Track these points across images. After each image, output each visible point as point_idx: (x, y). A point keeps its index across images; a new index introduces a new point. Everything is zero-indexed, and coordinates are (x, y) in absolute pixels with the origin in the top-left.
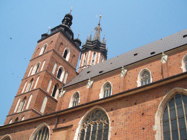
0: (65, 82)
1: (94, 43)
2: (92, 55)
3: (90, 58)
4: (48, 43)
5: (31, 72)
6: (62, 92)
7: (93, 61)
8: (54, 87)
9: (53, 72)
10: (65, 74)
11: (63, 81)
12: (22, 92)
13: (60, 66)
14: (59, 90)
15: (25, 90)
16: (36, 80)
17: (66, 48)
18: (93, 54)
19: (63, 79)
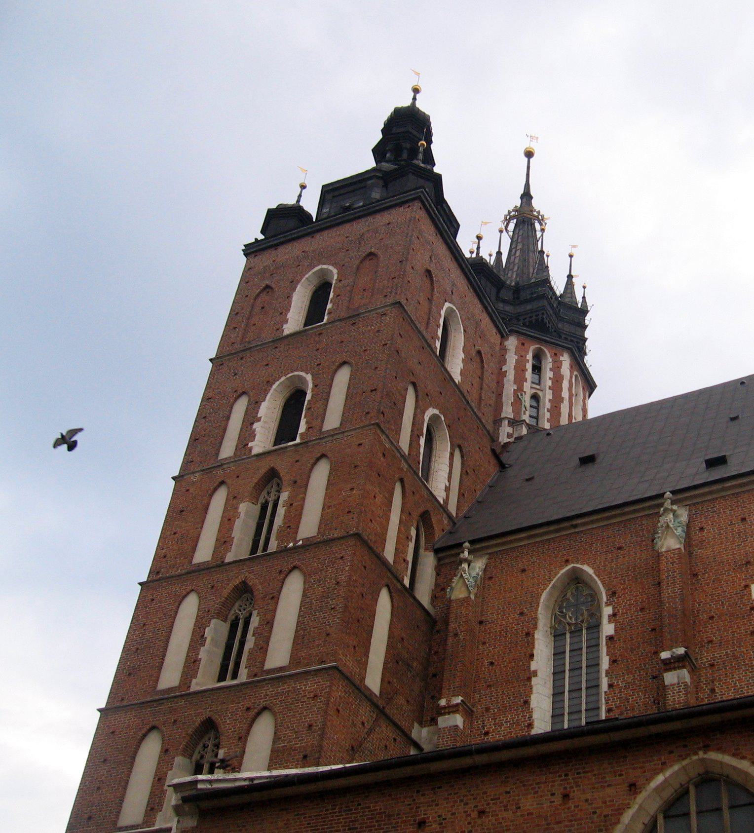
0: (452, 508)
1: (525, 295)
2: (529, 366)
3: (520, 379)
4: (341, 267)
5: (247, 434)
6: (465, 566)
7: (535, 397)
8: (413, 532)
9: (404, 443)
10: (452, 455)
11: (446, 501)
12: (204, 553)
13: (431, 412)
14: (437, 551)
15: (224, 541)
16: (301, 486)
17: (447, 305)
18: (530, 356)
19: (447, 489)
